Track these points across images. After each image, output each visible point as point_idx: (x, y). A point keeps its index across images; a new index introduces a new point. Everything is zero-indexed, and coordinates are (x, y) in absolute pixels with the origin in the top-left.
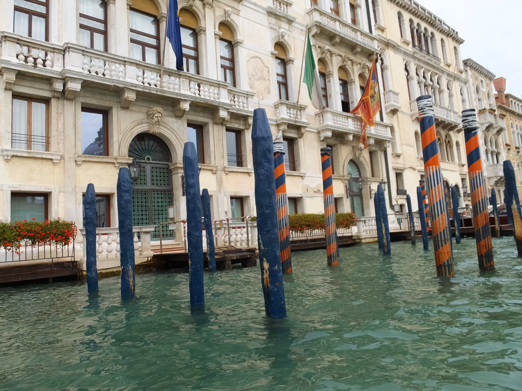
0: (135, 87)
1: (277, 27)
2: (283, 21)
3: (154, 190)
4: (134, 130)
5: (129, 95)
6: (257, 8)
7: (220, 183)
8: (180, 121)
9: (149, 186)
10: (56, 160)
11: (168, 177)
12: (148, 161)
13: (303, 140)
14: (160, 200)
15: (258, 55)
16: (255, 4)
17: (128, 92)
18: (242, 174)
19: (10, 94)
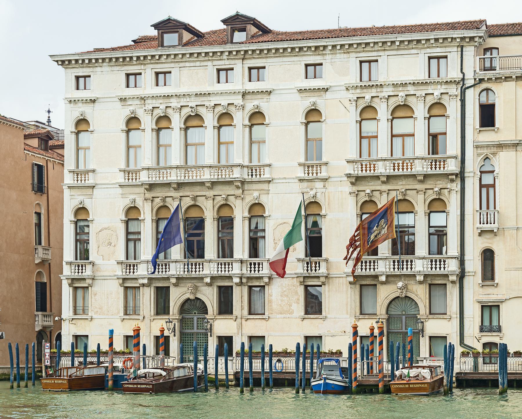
0: (174, 276)
1: (309, 190)
2: (317, 182)
3: (198, 333)
4: (181, 298)
5: (172, 280)
6: (287, 181)
7: (240, 327)
8: (211, 288)
9: (195, 330)
10: (142, 319)
11: (198, 326)
12: (195, 315)
13: (329, 285)
14: (202, 339)
15: (285, 221)
16: (285, 178)
17: (172, 279)
18: (260, 320)
19: (123, 288)
